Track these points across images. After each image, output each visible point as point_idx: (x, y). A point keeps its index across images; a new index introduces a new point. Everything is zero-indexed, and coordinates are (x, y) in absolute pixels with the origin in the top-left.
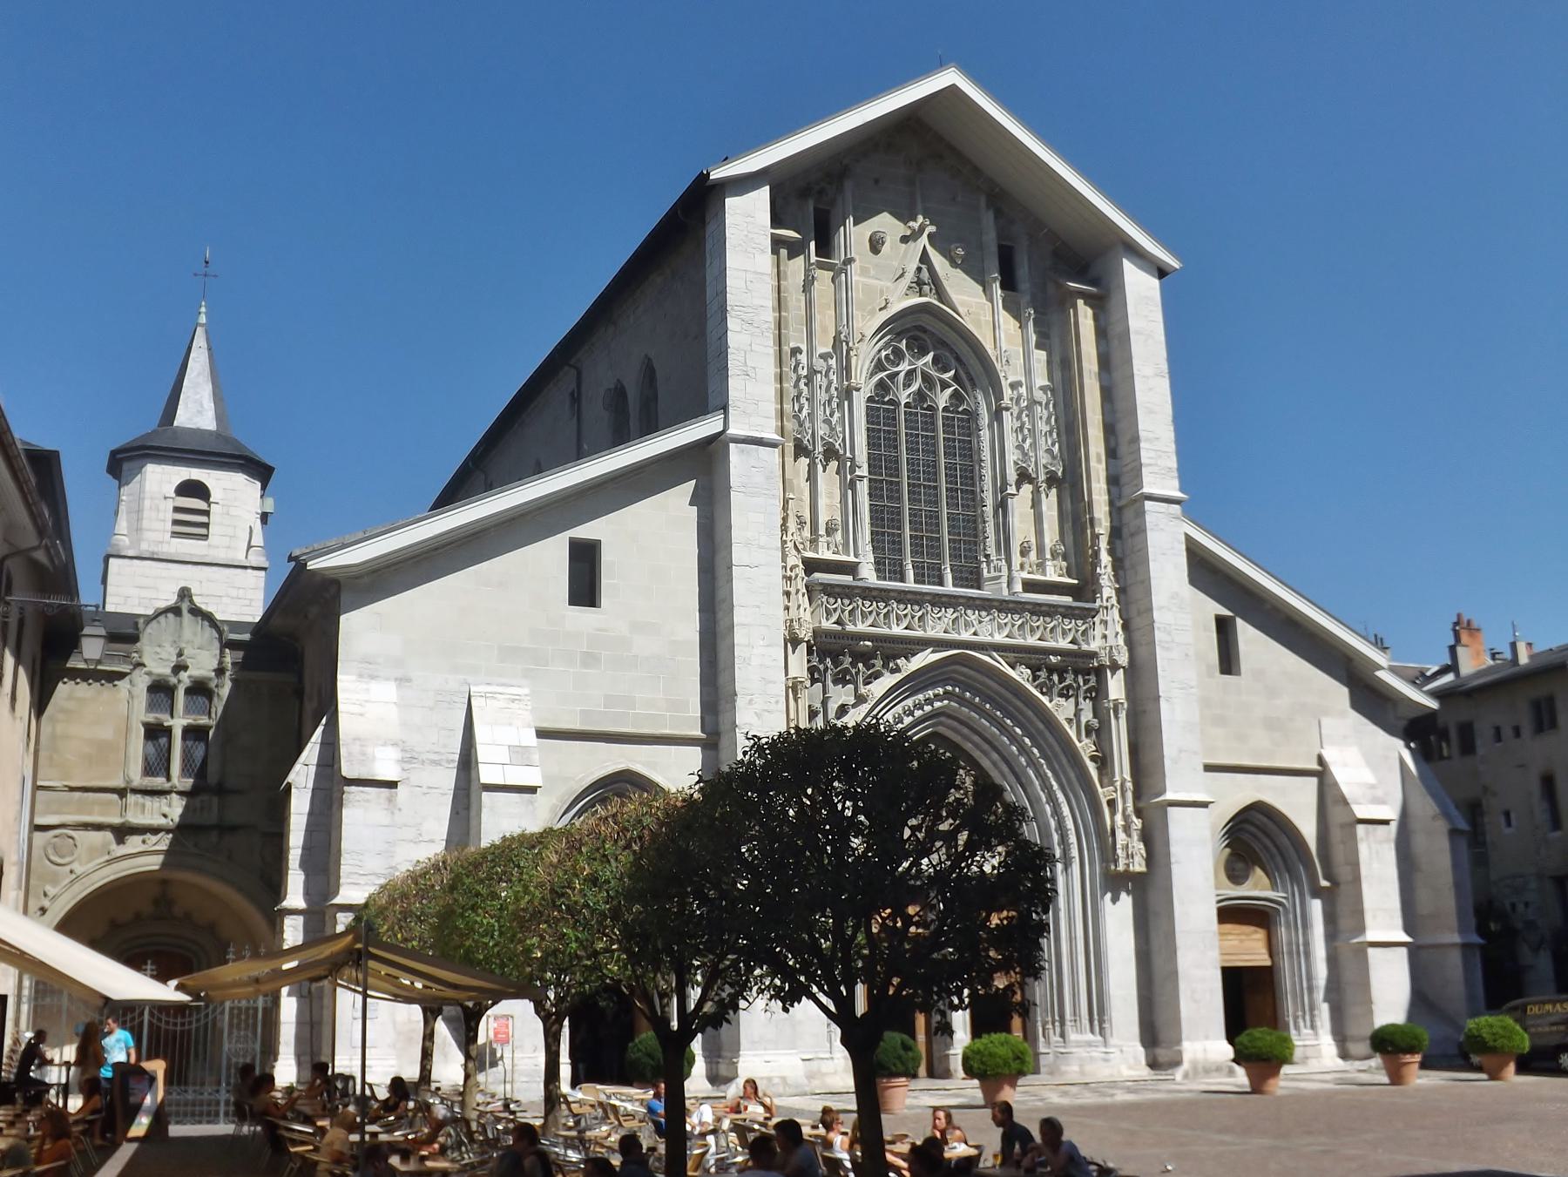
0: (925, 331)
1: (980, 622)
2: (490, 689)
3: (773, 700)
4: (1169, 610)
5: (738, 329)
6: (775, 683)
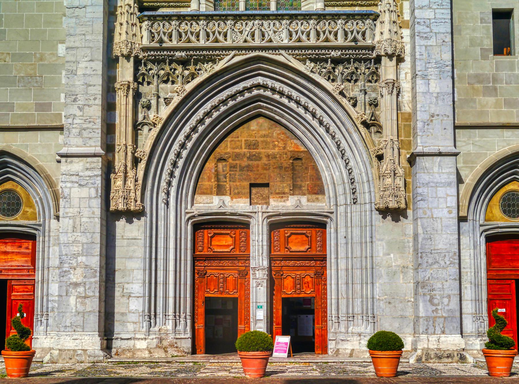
1: (275, 32)
3: (92, 98)
4: (430, 8)
6: (94, 86)
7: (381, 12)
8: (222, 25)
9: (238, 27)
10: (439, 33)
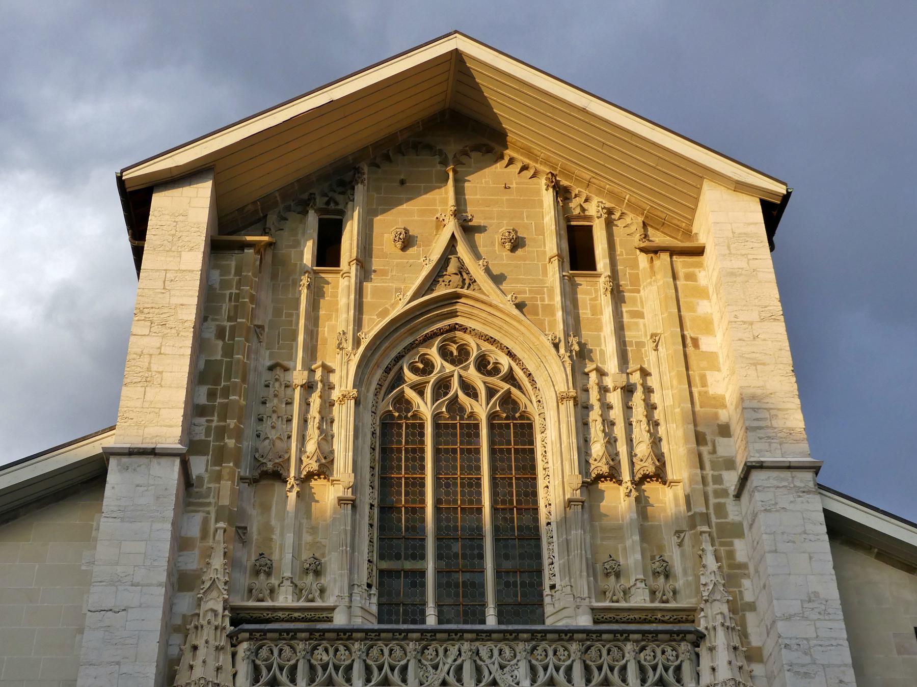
0: (464, 329)
1: (502, 667)
4: (806, 619)
5: (146, 332)
7: (706, 628)
8: (398, 652)
9: (430, 657)
10: (829, 666)
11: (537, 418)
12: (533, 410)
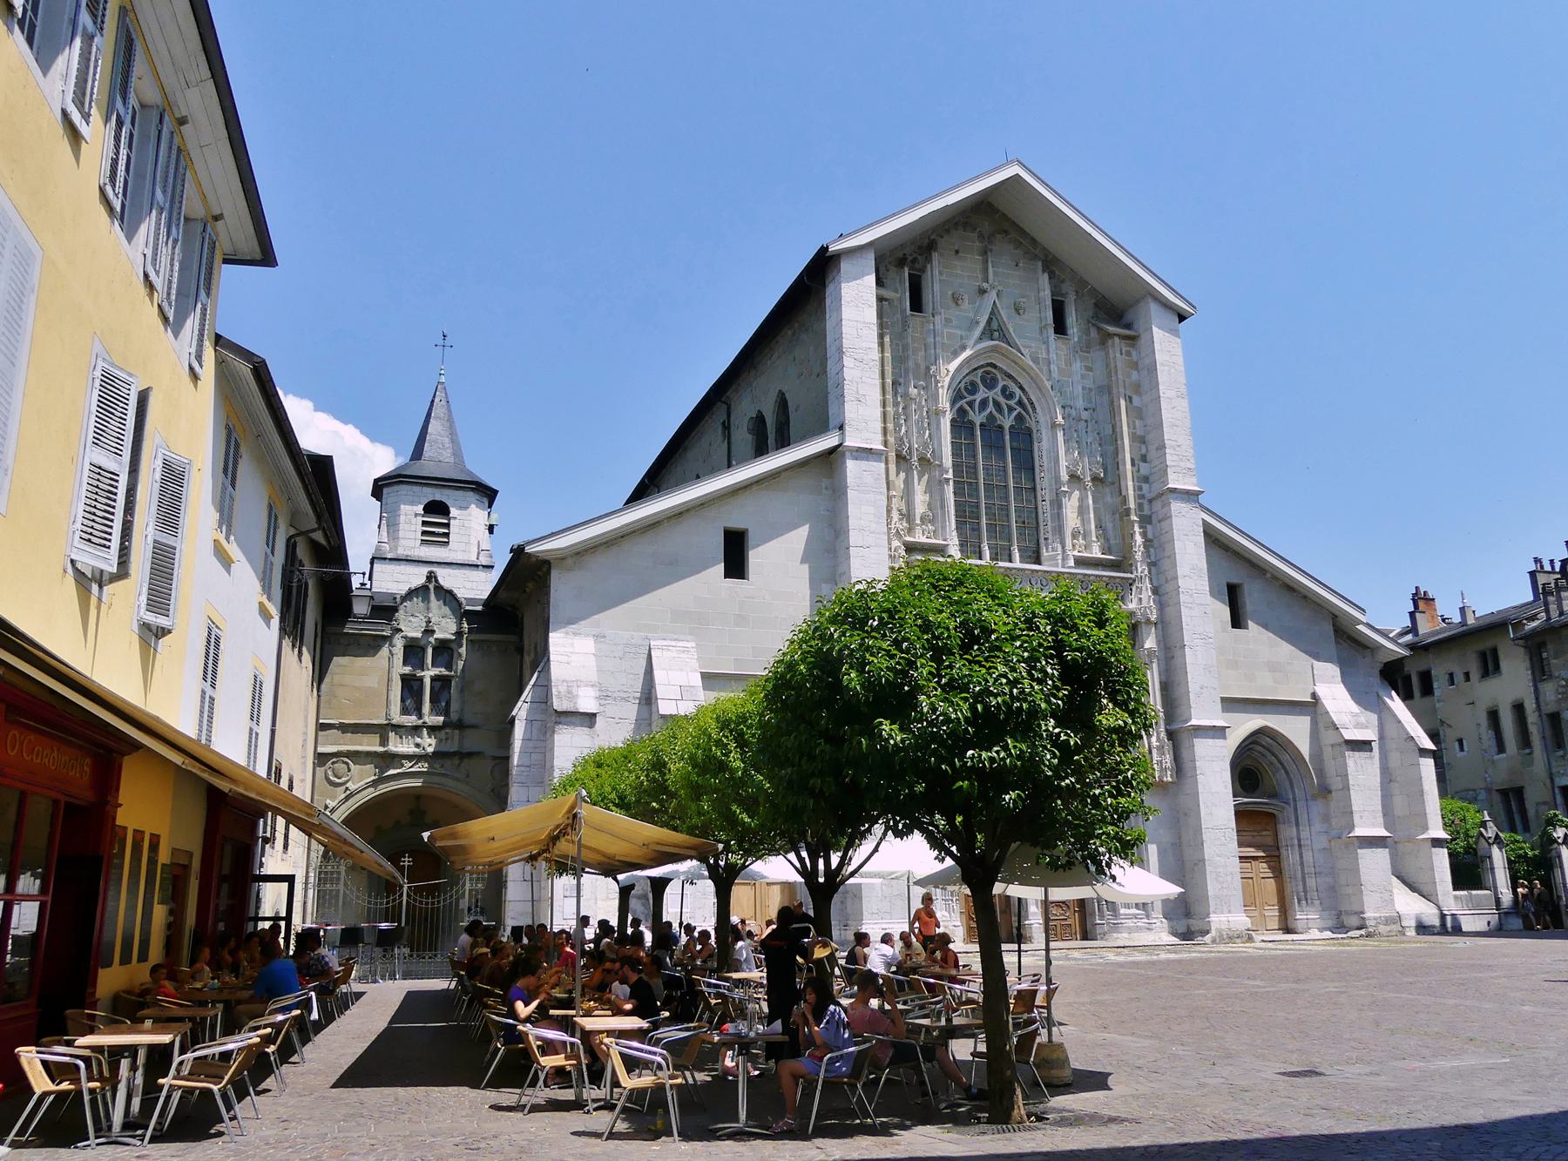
0: (995, 366)
2: (665, 643)
11: (1035, 431)
12: (1033, 425)
